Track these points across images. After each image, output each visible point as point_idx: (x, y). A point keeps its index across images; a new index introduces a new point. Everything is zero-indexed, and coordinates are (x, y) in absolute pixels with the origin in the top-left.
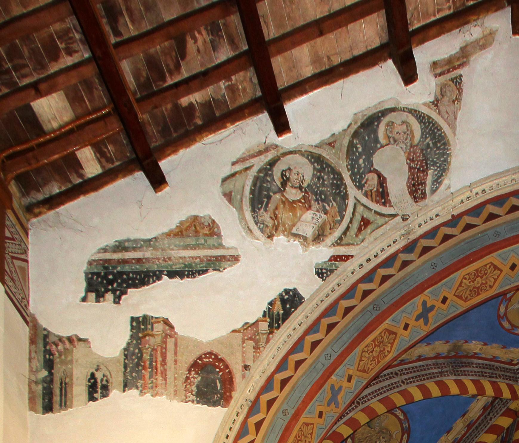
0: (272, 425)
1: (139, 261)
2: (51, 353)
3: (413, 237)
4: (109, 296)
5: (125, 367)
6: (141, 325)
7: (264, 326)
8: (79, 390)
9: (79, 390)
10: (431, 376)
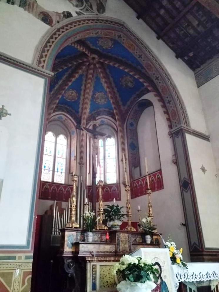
0: (63, 37)
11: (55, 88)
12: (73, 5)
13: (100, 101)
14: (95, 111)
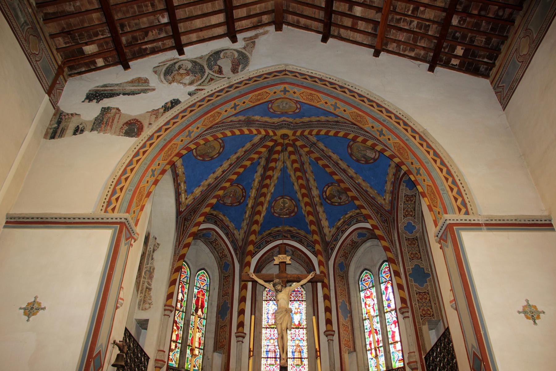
0: (158, 145)
1: (111, 90)
2: (61, 119)
3: (231, 84)
4: (95, 101)
5: (94, 124)
6: (105, 110)
7: (162, 111)
8: (70, 130)
9: (70, 130)
10: (236, 127)
11: (250, 206)
12: (185, 84)
13: (340, 199)
14: (339, 220)
